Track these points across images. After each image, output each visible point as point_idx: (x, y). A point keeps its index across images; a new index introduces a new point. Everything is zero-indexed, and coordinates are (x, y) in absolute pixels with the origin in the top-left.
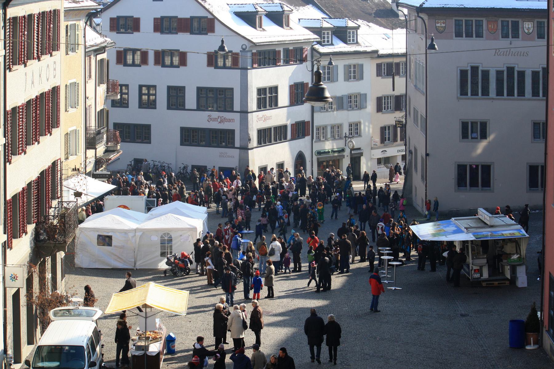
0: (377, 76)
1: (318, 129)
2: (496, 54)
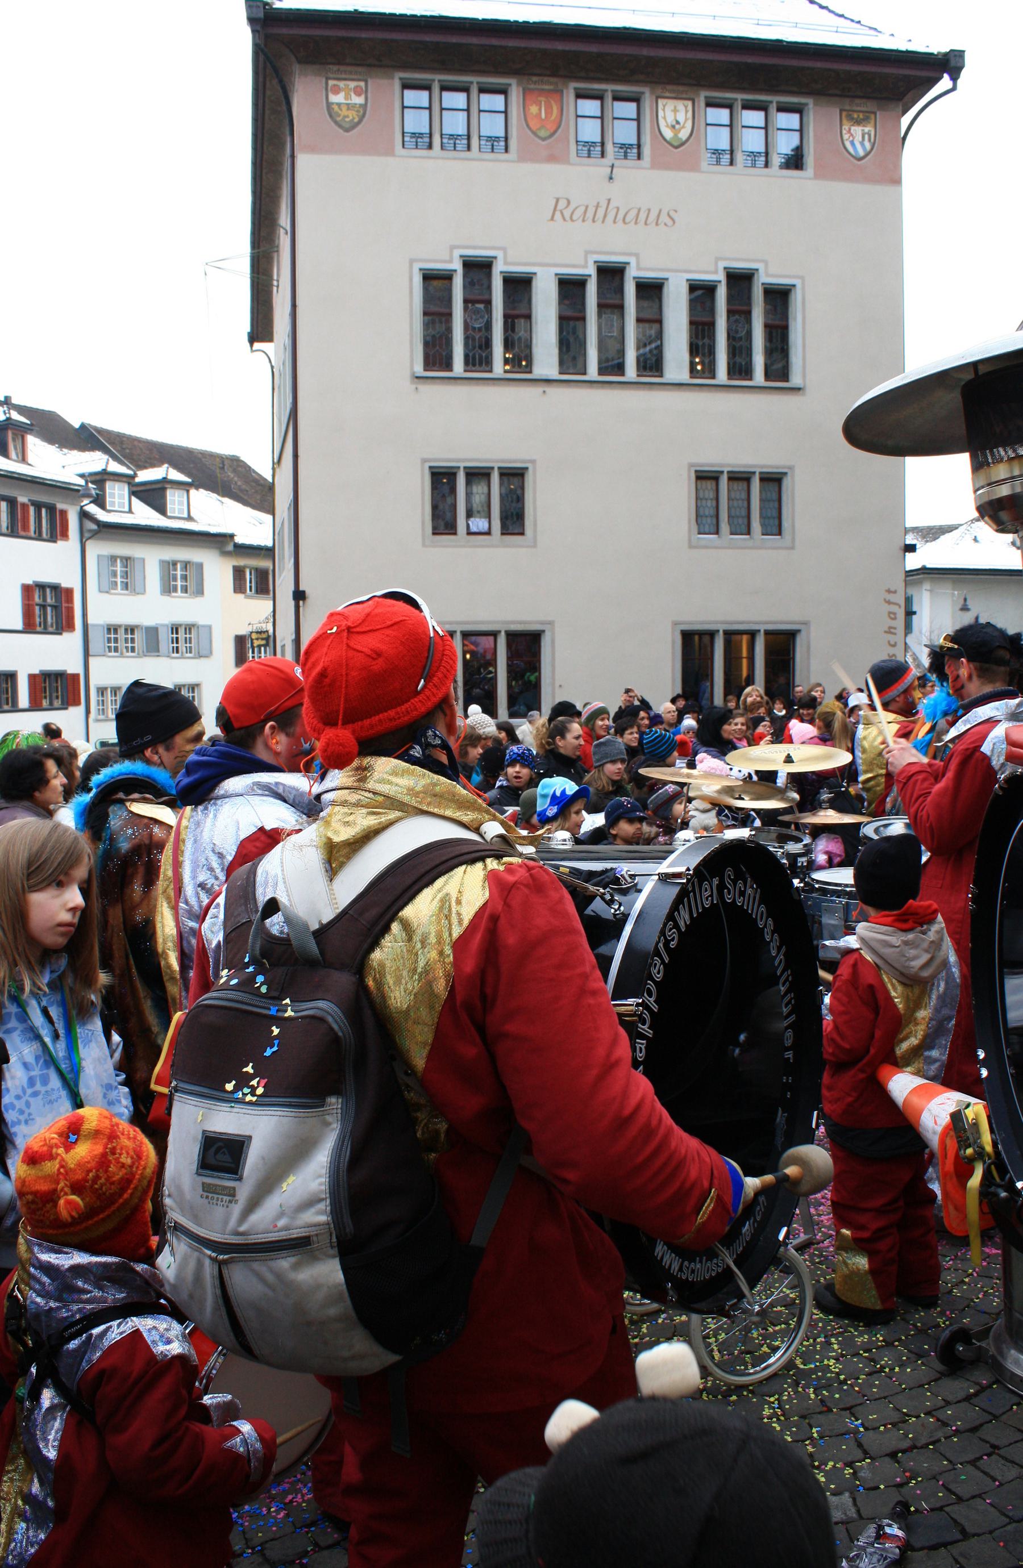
0: (235, 591)
1: (102, 691)
2: (558, 215)
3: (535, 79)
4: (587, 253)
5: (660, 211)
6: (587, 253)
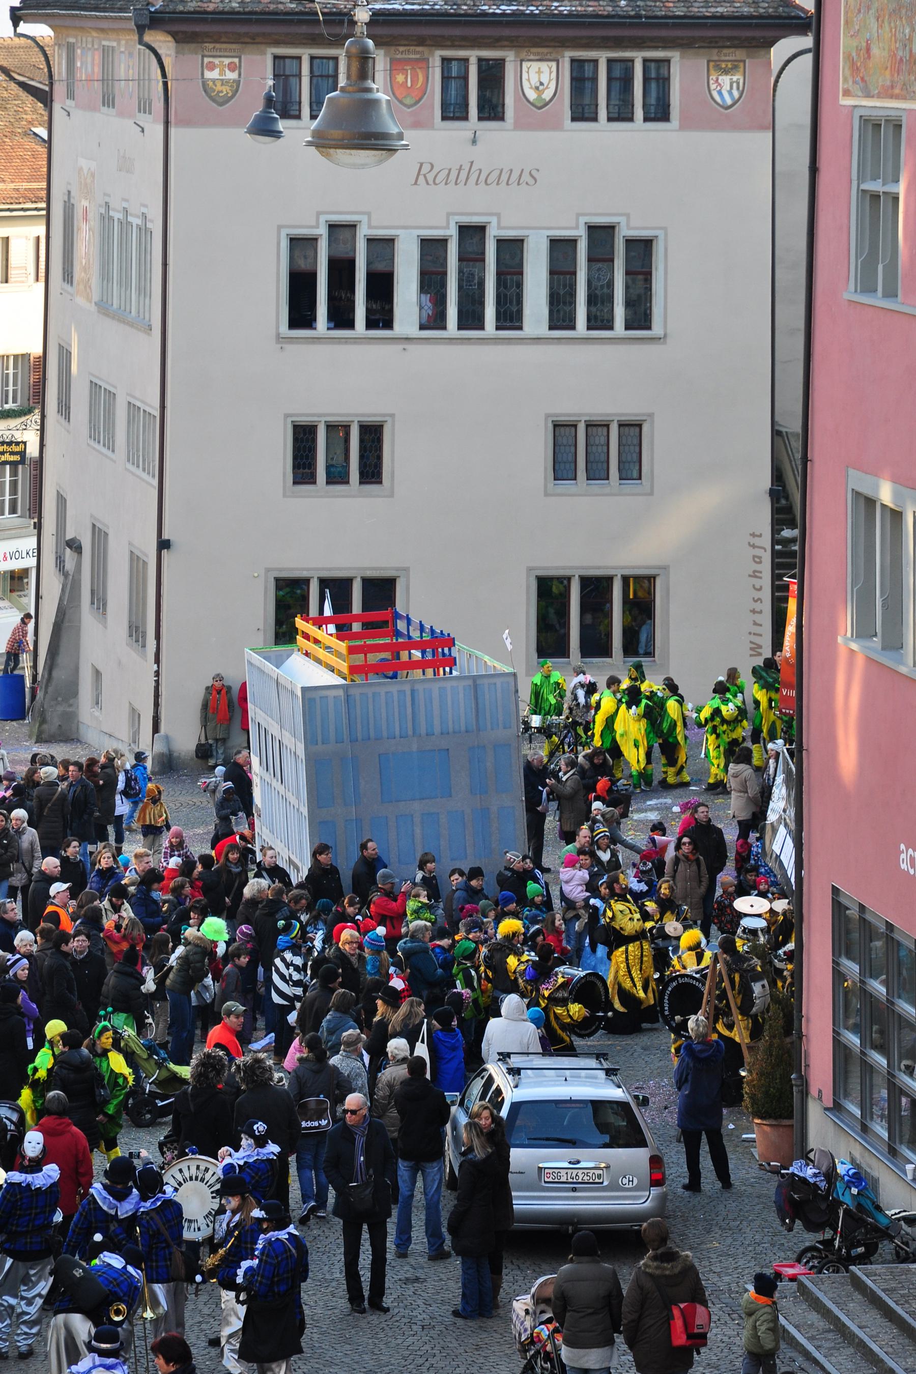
2: (421, 178)
3: (401, 49)
4: (449, 215)
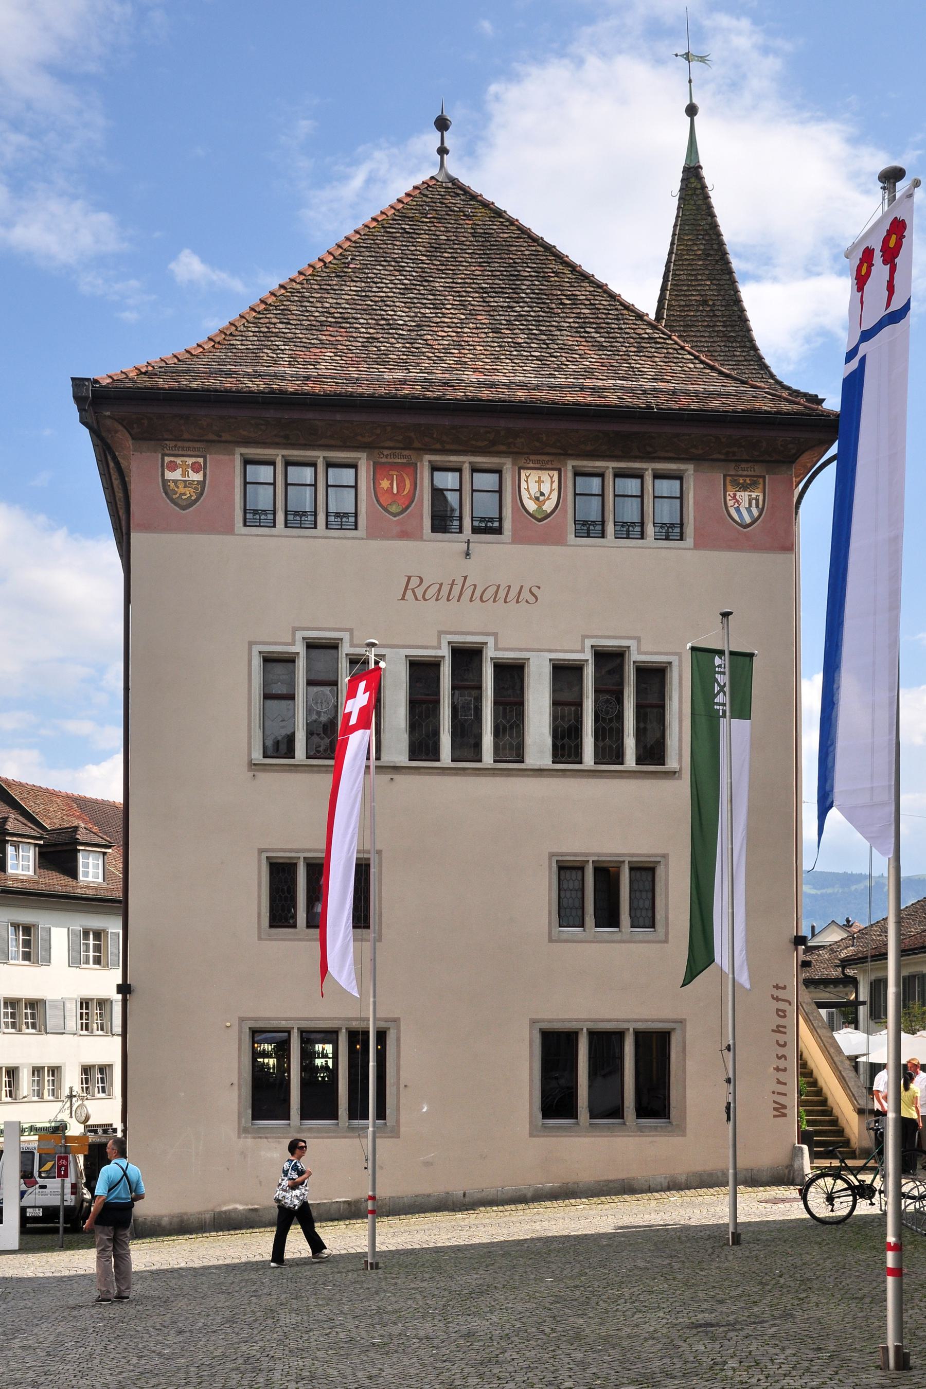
2: (409, 592)
3: (386, 452)
4: (440, 633)
5: (522, 587)
6: (440, 633)
